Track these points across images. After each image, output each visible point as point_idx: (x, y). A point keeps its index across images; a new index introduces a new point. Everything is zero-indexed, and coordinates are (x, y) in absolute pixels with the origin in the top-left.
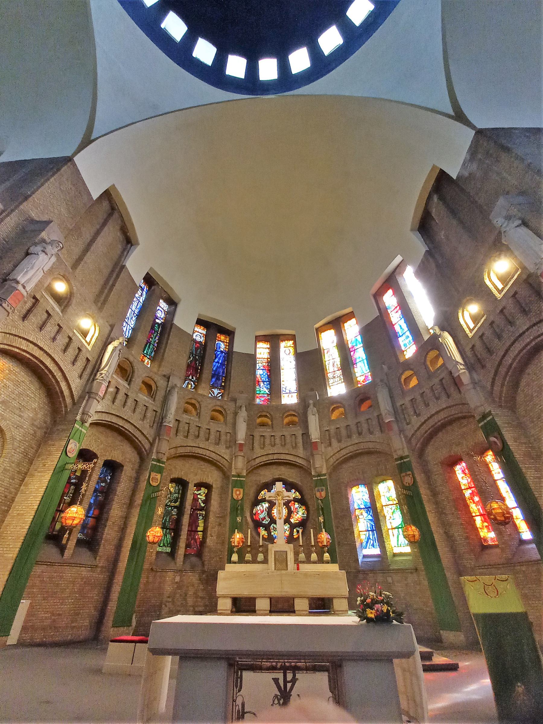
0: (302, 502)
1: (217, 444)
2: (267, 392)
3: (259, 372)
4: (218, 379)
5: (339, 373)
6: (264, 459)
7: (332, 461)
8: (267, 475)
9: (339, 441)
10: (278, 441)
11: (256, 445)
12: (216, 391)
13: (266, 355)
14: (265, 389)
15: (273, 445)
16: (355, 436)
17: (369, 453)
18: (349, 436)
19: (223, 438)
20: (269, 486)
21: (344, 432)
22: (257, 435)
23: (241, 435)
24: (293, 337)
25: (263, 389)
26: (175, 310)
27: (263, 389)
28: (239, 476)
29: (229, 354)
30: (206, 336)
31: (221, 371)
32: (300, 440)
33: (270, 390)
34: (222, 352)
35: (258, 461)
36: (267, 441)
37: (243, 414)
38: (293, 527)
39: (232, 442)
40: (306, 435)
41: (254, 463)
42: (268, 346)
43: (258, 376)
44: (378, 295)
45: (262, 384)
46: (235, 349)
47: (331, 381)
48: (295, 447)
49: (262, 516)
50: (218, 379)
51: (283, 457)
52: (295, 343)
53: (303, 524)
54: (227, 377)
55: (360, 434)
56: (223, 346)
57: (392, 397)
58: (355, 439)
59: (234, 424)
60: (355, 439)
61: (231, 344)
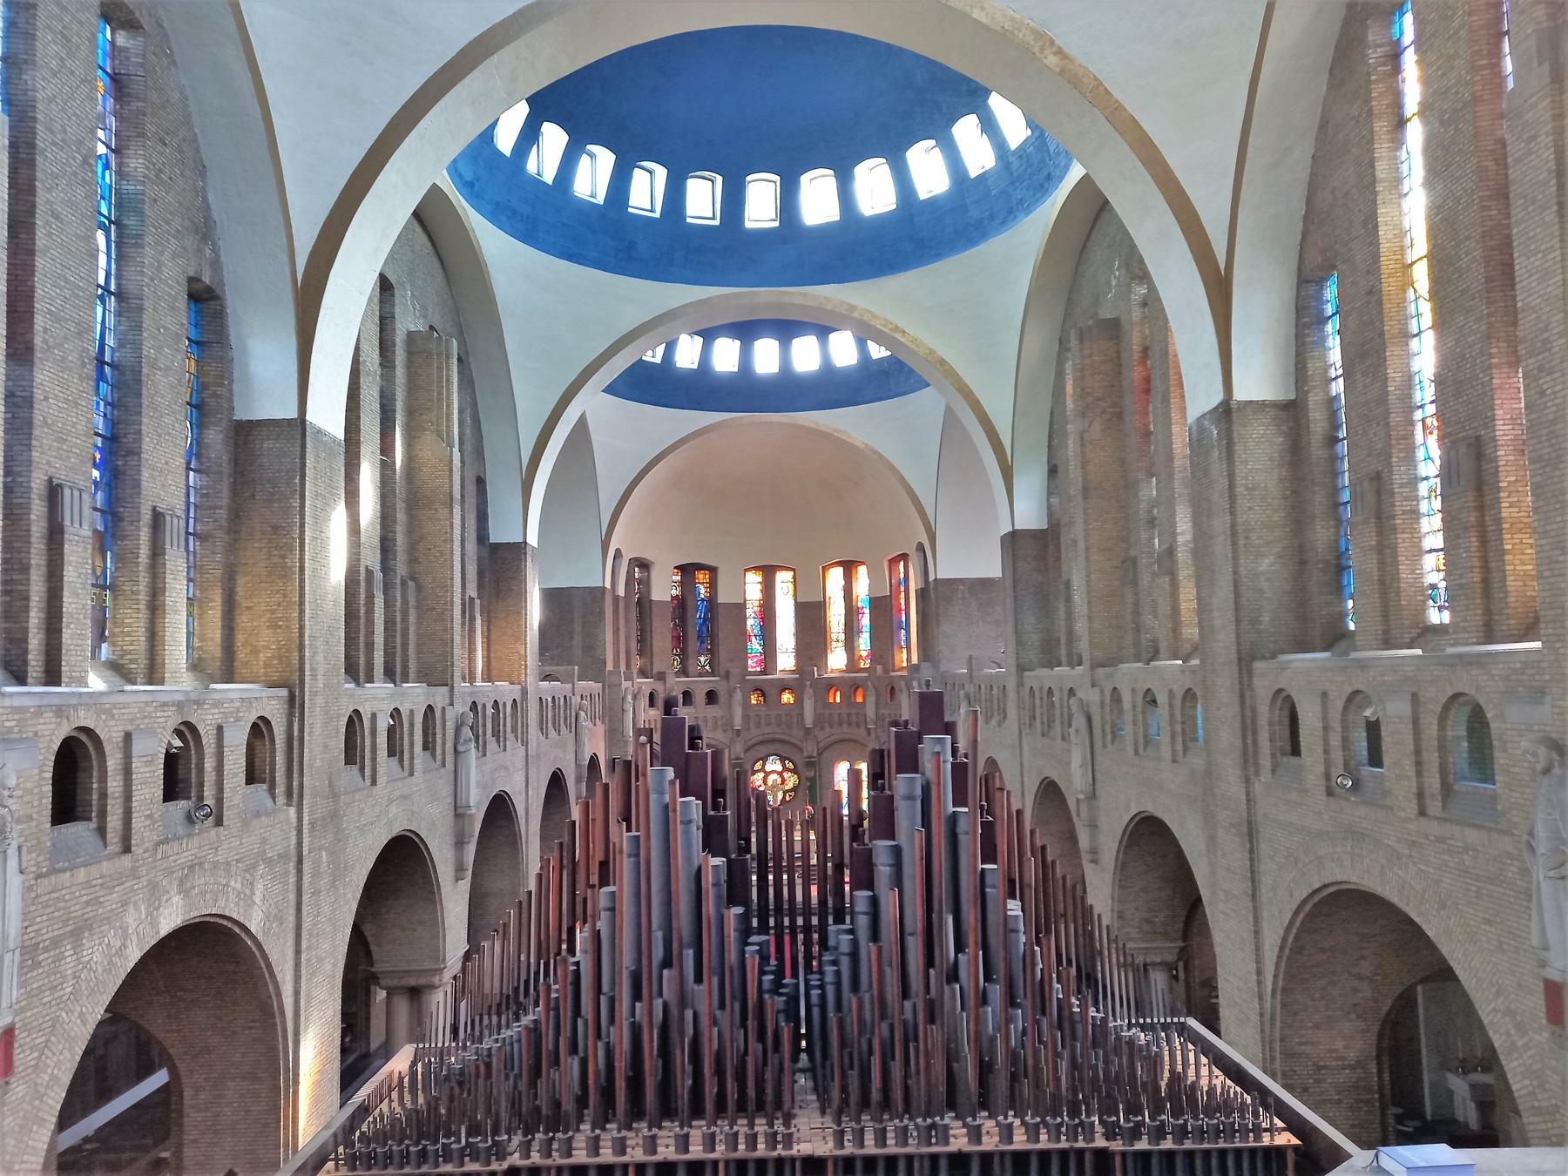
0: (794, 771)
1: (715, 728)
2: (760, 649)
3: (750, 622)
4: (702, 642)
5: (842, 637)
6: (761, 738)
7: (822, 745)
8: (763, 750)
9: (831, 727)
10: (773, 720)
11: (752, 725)
12: (702, 659)
13: (758, 595)
14: (758, 647)
15: (770, 724)
16: (845, 726)
17: (855, 741)
18: (840, 724)
19: (720, 723)
20: (765, 759)
21: (836, 718)
22: (752, 715)
23: (738, 722)
24: (793, 570)
25: (755, 646)
26: (649, 576)
27: (755, 646)
28: (737, 759)
29: (711, 601)
30: (682, 583)
31: (704, 629)
32: (795, 720)
33: (764, 646)
34: (703, 600)
35: (754, 741)
36: (763, 721)
37: (738, 696)
38: (785, 793)
39: (728, 725)
40: (801, 715)
41: (750, 743)
42: (760, 579)
43: (749, 628)
44: (893, 562)
45: (753, 639)
46: (720, 601)
47: (834, 644)
48: (789, 727)
49: (758, 784)
50: (702, 642)
51: (778, 736)
52: (794, 578)
53: (794, 789)
54: (713, 636)
55: (850, 724)
56: (703, 591)
57: (877, 704)
58: (845, 728)
59: (730, 706)
60: (845, 728)
61: (713, 585)
